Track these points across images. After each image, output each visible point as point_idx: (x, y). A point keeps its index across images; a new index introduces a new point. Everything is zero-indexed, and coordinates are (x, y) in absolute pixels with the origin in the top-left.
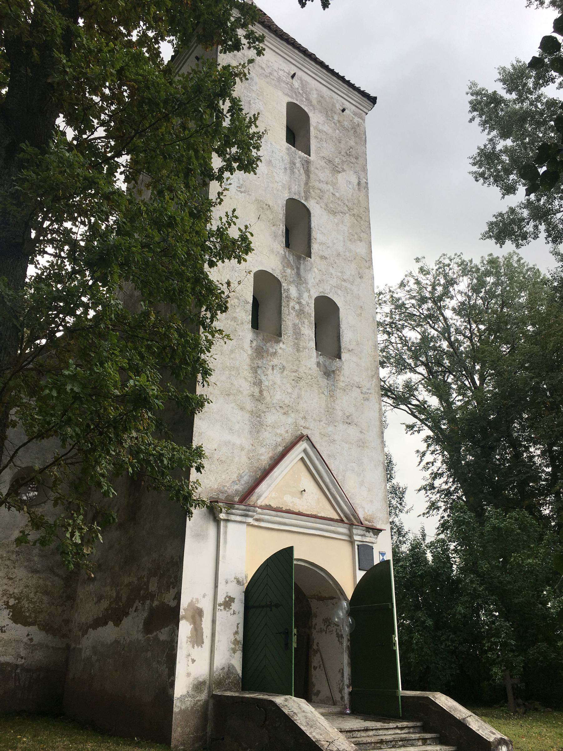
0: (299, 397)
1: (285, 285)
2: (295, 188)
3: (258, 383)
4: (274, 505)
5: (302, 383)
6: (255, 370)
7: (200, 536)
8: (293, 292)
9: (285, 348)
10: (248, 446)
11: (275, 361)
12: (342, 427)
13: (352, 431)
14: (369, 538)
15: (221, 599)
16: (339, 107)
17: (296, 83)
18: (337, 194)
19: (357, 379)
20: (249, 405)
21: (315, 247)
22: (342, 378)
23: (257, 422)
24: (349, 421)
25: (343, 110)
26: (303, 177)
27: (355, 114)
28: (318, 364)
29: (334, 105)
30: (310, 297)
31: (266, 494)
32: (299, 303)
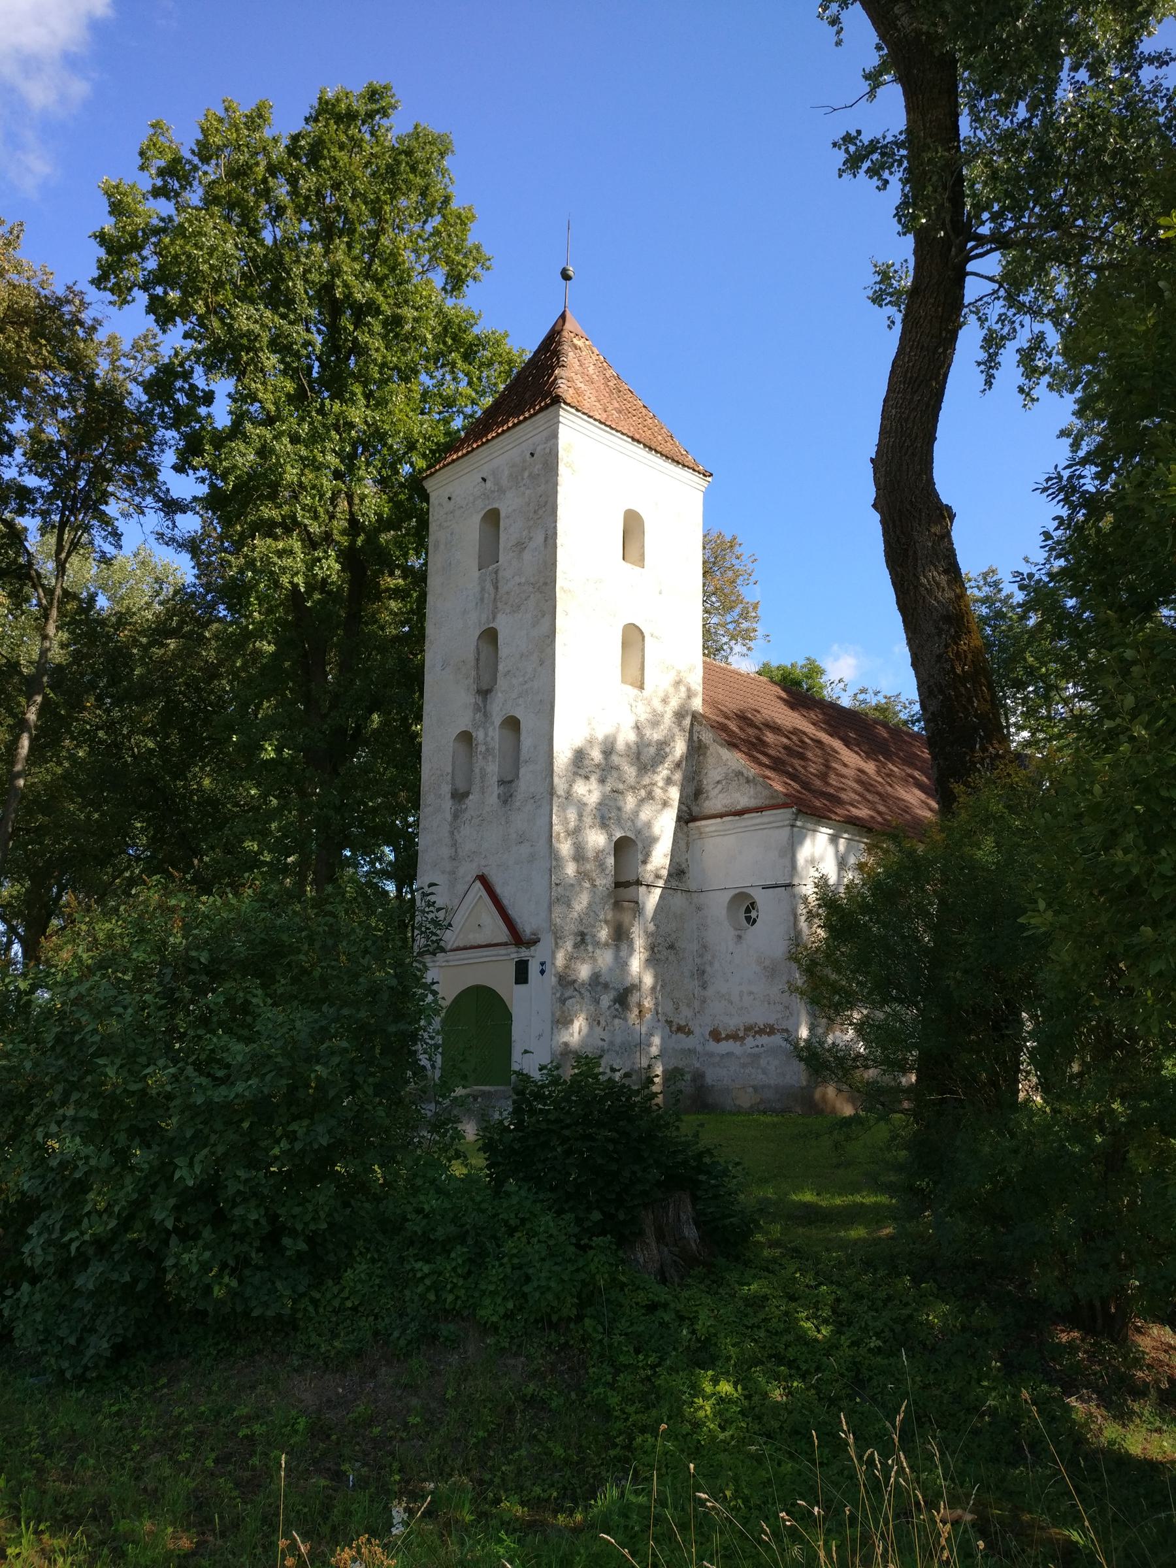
2: (484, 617)
3: (454, 844)
4: (461, 945)
6: (452, 833)
14: (524, 953)
17: (489, 484)
22: (519, 797)
24: (522, 839)
25: (532, 455)
29: (524, 461)
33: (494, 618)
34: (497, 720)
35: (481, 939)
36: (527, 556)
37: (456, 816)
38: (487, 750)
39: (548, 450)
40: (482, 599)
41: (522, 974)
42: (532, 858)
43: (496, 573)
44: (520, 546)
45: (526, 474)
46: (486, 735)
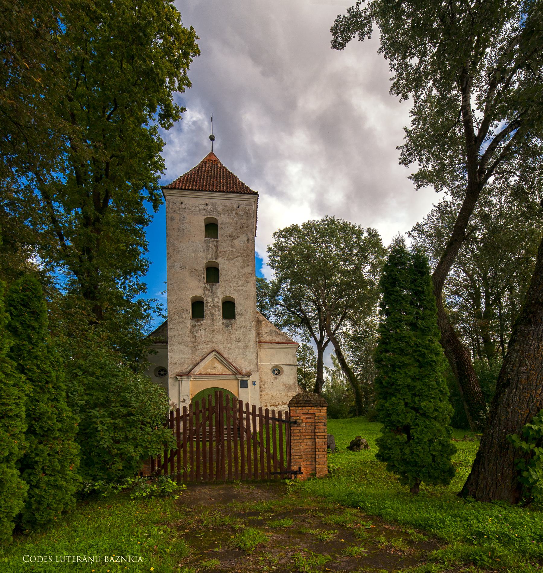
0: (213, 337)
1: (205, 298)
2: (209, 256)
5: (215, 332)
6: (192, 333)
7: (173, 385)
8: (210, 299)
9: (206, 321)
10: (191, 357)
11: (201, 327)
12: (235, 343)
13: (241, 344)
14: (245, 378)
15: (181, 400)
16: (235, 206)
17: (209, 207)
18: (234, 250)
19: (244, 324)
20: (191, 345)
21: (221, 278)
23: (194, 349)
24: (239, 340)
26: (215, 250)
27: (247, 205)
28: (223, 323)
29: (233, 207)
30: (219, 299)
31: (198, 370)
32: (213, 303)
33: (216, 259)
34: (221, 297)
35: (214, 372)
36: (237, 242)
37: (194, 326)
38: (214, 306)
39: (247, 209)
40: (208, 250)
41: (244, 384)
42: (245, 347)
43: (217, 242)
44: (232, 238)
45: (234, 213)
46: (213, 300)
